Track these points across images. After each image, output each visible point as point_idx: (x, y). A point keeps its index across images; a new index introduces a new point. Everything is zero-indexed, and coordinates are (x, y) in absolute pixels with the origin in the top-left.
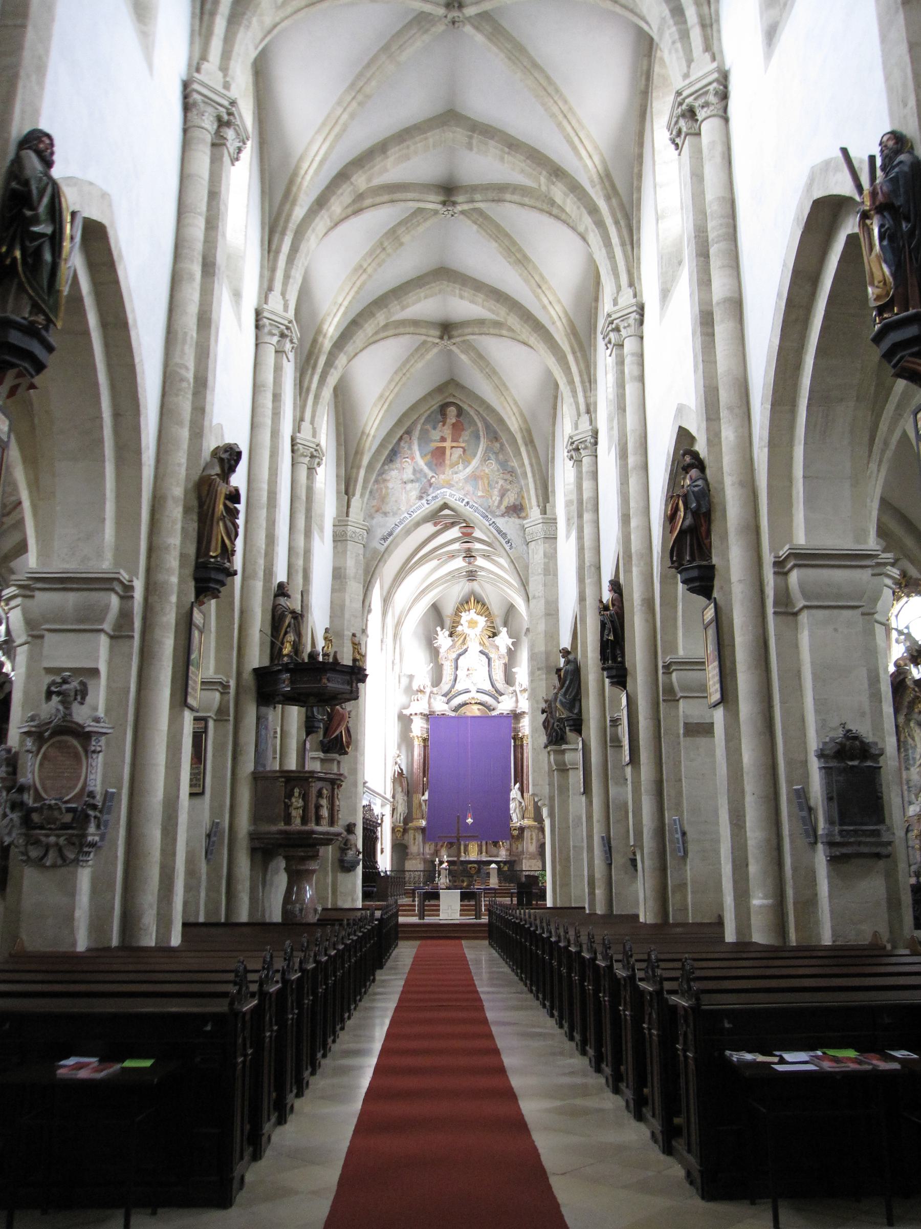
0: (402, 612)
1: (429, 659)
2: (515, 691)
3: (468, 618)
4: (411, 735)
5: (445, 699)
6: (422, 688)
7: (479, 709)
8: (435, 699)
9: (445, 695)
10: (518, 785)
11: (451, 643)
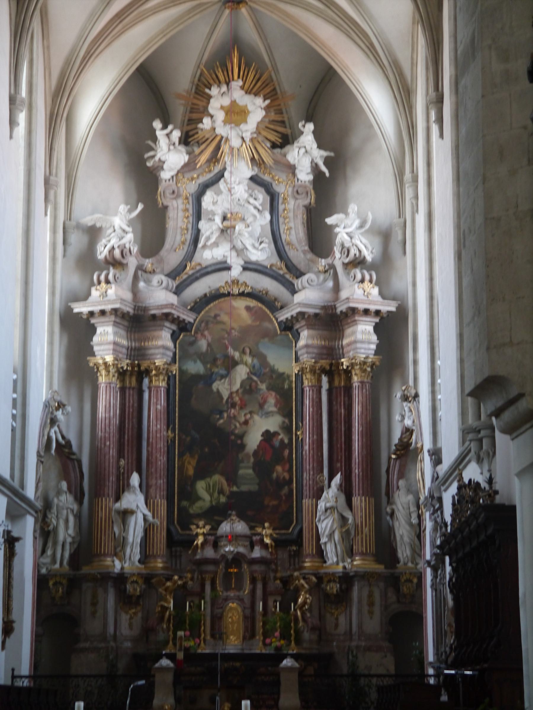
0: (68, 63)
1: (134, 196)
2: (332, 267)
3: (226, 101)
4: (92, 361)
5: (173, 284)
6: (117, 253)
7: (248, 308)
8: (148, 282)
9: (173, 275)
10: (337, 479)
11: (187, 158)
